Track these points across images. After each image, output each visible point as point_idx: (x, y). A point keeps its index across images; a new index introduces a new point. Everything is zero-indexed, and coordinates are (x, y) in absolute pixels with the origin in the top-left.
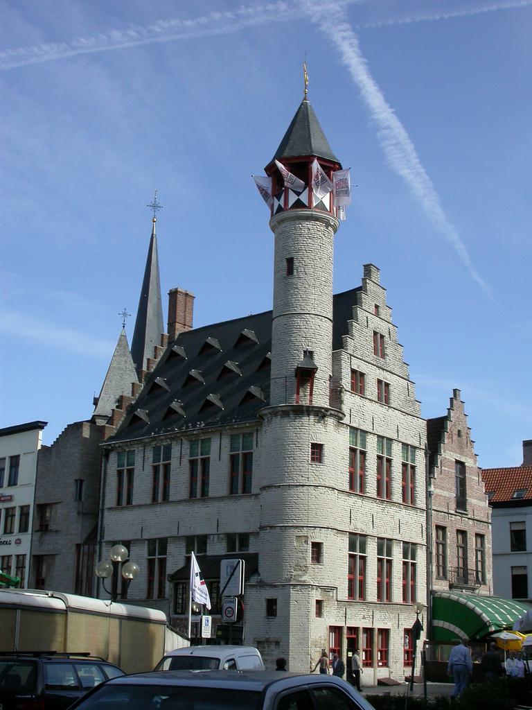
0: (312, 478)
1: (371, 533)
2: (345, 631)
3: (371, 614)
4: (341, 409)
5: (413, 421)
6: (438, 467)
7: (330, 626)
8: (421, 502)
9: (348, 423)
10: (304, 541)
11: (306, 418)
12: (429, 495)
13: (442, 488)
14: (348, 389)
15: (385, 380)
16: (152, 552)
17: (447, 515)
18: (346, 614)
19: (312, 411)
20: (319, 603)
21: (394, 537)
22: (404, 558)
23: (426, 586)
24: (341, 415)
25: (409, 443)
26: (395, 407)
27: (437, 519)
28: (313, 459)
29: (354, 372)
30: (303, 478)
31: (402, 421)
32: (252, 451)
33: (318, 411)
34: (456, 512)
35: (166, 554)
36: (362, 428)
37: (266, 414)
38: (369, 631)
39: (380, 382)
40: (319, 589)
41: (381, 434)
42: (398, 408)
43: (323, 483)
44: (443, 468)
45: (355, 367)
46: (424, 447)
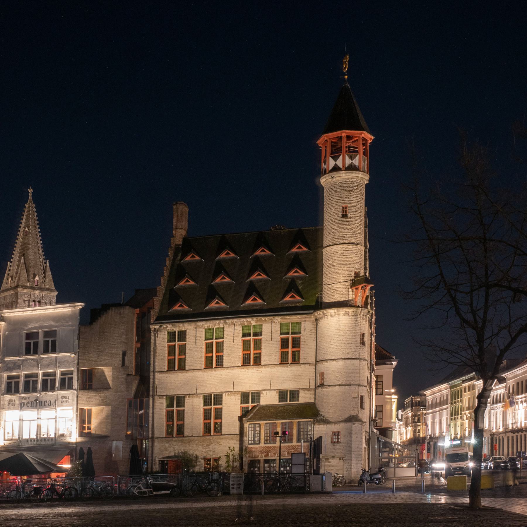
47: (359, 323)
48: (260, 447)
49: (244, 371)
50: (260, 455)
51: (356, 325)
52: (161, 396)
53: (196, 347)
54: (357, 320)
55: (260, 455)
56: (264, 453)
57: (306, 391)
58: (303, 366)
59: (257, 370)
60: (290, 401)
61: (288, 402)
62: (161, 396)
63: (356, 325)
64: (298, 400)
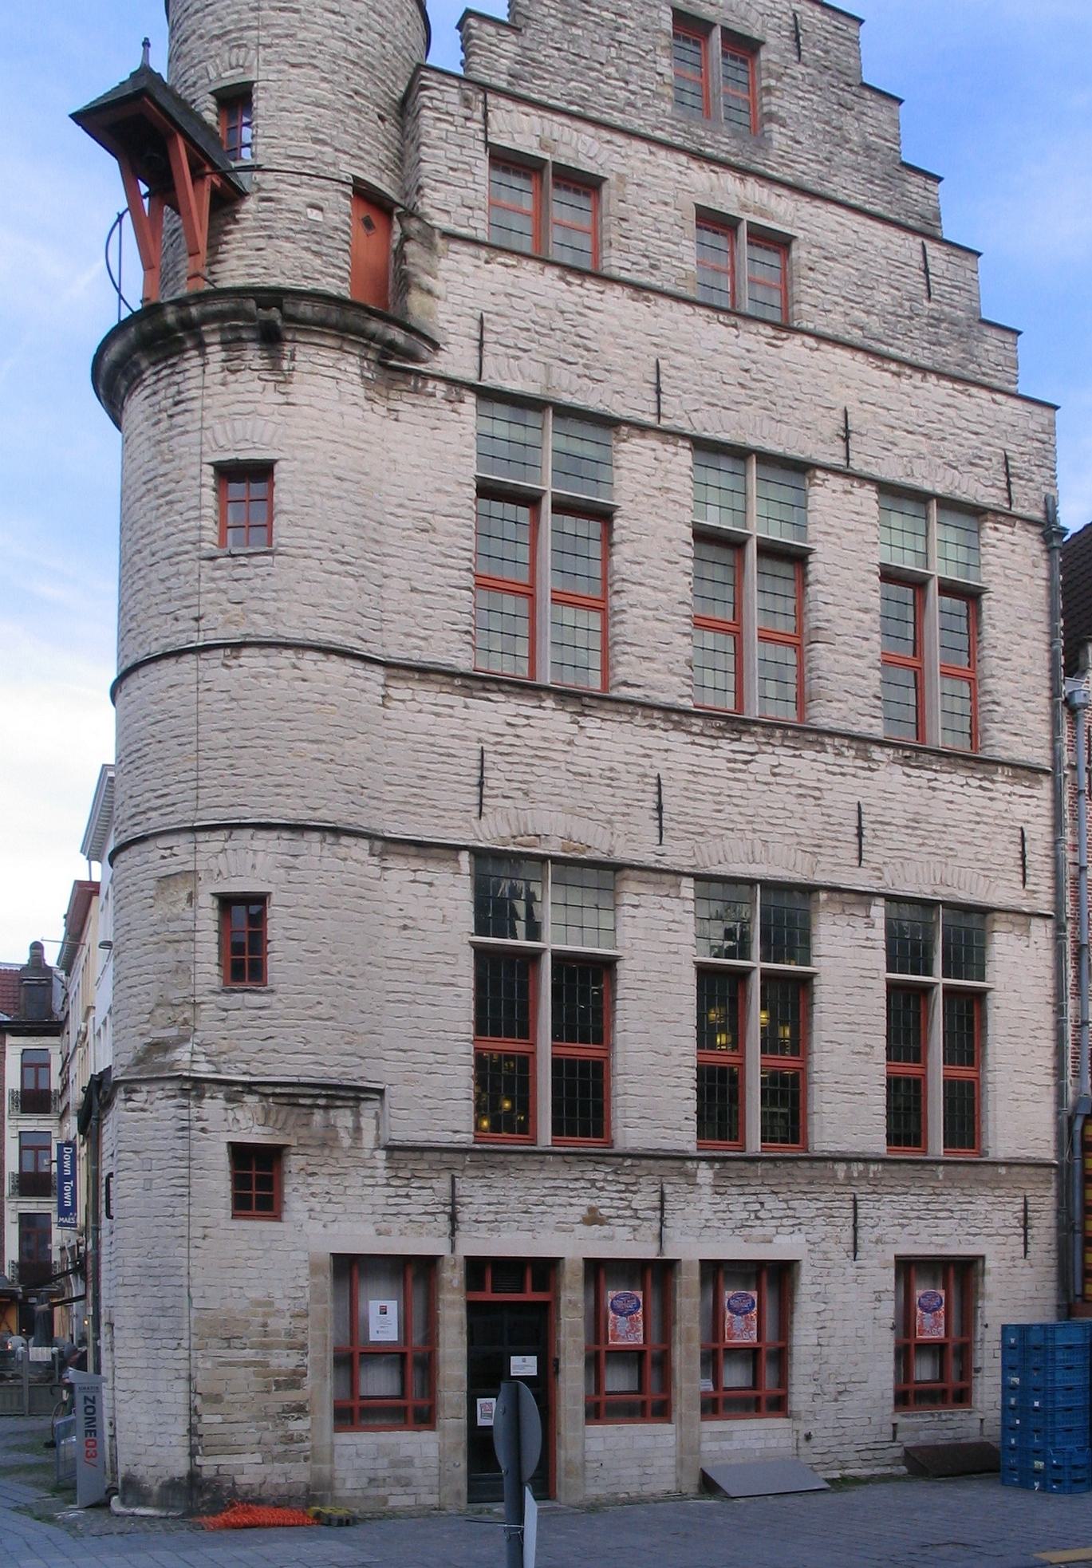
0: (213, 617)
1: (649, 860)
2: (453, 1277)
3: (644, 1199)
4: (406, 312)
7: (337, 1258)
9: (470, 376)
10: (184, 895)
15: (748, 217)
18: (453, 1204)
19: (206, 319)
21: (821, 878)
23: (1050, 1081)
31: (877, 395)
39: (713, 221)
43: (265, 629)
54: (183, 387)
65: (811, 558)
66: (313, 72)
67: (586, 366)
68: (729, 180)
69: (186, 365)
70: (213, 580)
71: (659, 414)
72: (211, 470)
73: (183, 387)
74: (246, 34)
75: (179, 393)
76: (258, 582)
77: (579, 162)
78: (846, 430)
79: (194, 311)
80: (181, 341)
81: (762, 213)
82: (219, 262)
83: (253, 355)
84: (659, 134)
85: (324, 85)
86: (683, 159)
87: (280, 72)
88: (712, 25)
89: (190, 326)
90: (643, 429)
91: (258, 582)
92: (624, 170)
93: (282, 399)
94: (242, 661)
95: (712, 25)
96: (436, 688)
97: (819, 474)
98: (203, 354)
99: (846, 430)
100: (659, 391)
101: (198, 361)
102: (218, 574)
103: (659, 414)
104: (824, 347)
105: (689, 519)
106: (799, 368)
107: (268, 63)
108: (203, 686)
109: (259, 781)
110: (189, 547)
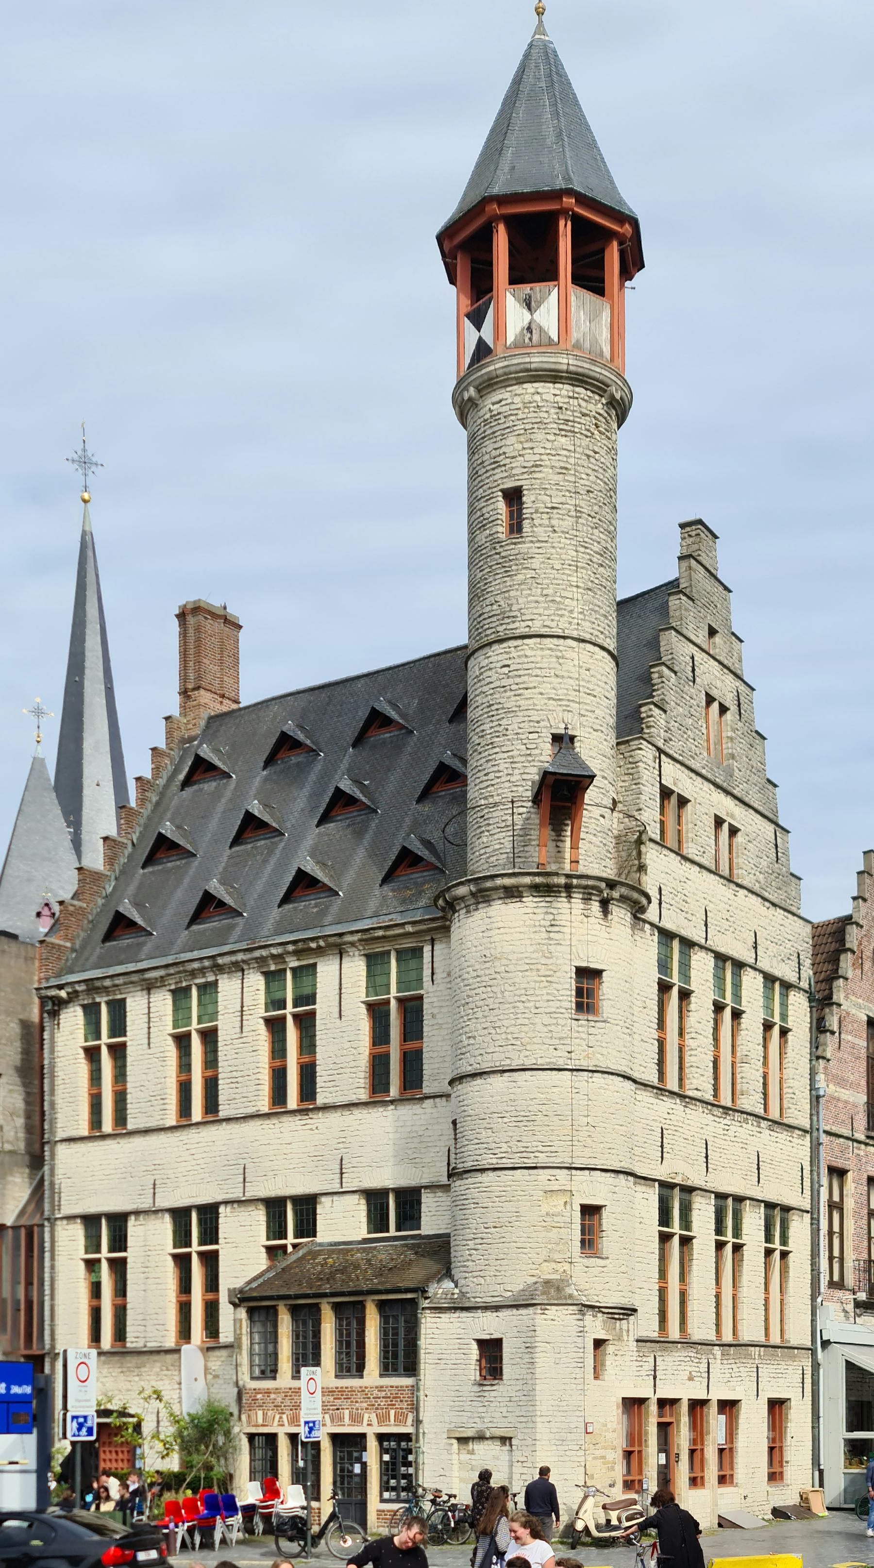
5: (786, 922)
6: (833, 1033)
8: (800, 1115)
11: (562, 903)
12: (816, 1099)
13: (841, 1082)
14: (653, 836)
15: (729, 820)
16: (182, 1236)
17: (850, 1143)
20: (599, 1344)
22: (766, 1242)
24: (644, 901)
25: (777, 973)
26: (750, 885)
27: (828, 1156)
28: (580, 1007)
29: (666, 793)
30: (558, 1053)
32: (422, 992)
33: (593, 887)
34: (868, 1137)
35: (217, 1243)
36: (684, 933)
37: (462, 898)
38: (697, 1406)
39: (719, 822)
40: (600, 1315)
41: (722, 950)
42: (757, 888)
43: (603, 1065)
44: (843, 1036)
45: (668, 782)
46: (806, 986)
47: (567, 930)
48: (277, 1391)
49: (272, 1126)
50: (277, 1417)
51: (550, 939)
52: (70, 1218)
53: (149, 1051)
55: (277, 1417)
56: (288, 1412)
57: (440, 1194)
58: (428, 1103)
59: (304, 1122)
60: (398, 1229)
61: (393, 1232)
62: (70, 1218)
63: (550, 939)
64: (419, 1228)
65: (744, 1016)
66: (601, 735)
67: (687, 913)
68: (722, 796)
69: (559, 905)
70: (578, 1032)
71: (706, 939)
72: (574, 969)
73: (557, 917)
74: (572, 704)
75: (554, 920)
76: (599, 1037)
77: (683, 790)
78: (756, 943)
79: (575, 881)
80: (560, 892)
81: (732, 816)
82: (562, 841)
83: (595, 906)
84: (704, 772)
85: (605, 743)
86: (712, 787)
87: (590, 733)
88: (715, 700)
89: (568, 888)
90: (701, 947)
91: (599, 1037)
92: (696, 796)
93: (608, 936)
94: (594, 1080)
95: (715, 700)
96: (649, 1094)
97: (748, 969)
98: (569, 902)
99: (756, 943)
100: (706, 925)
101: (567, 905)
102: (580, 1029)
103: (706, 939)
104: (750, 895)
105: (713, 997)
106: (742, 908)
107: (584, 726)
108: (574, 1091)
109: (602, 1145)
110: (563, 1011)
